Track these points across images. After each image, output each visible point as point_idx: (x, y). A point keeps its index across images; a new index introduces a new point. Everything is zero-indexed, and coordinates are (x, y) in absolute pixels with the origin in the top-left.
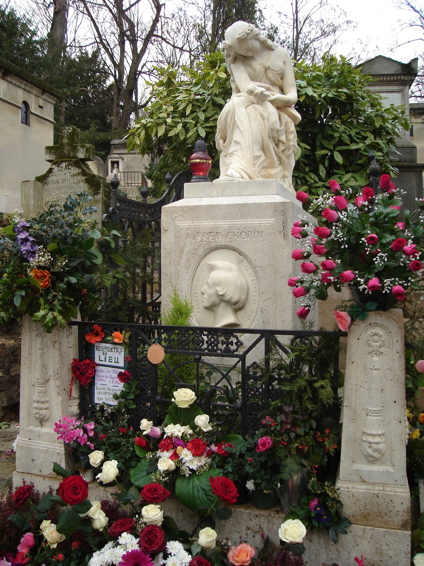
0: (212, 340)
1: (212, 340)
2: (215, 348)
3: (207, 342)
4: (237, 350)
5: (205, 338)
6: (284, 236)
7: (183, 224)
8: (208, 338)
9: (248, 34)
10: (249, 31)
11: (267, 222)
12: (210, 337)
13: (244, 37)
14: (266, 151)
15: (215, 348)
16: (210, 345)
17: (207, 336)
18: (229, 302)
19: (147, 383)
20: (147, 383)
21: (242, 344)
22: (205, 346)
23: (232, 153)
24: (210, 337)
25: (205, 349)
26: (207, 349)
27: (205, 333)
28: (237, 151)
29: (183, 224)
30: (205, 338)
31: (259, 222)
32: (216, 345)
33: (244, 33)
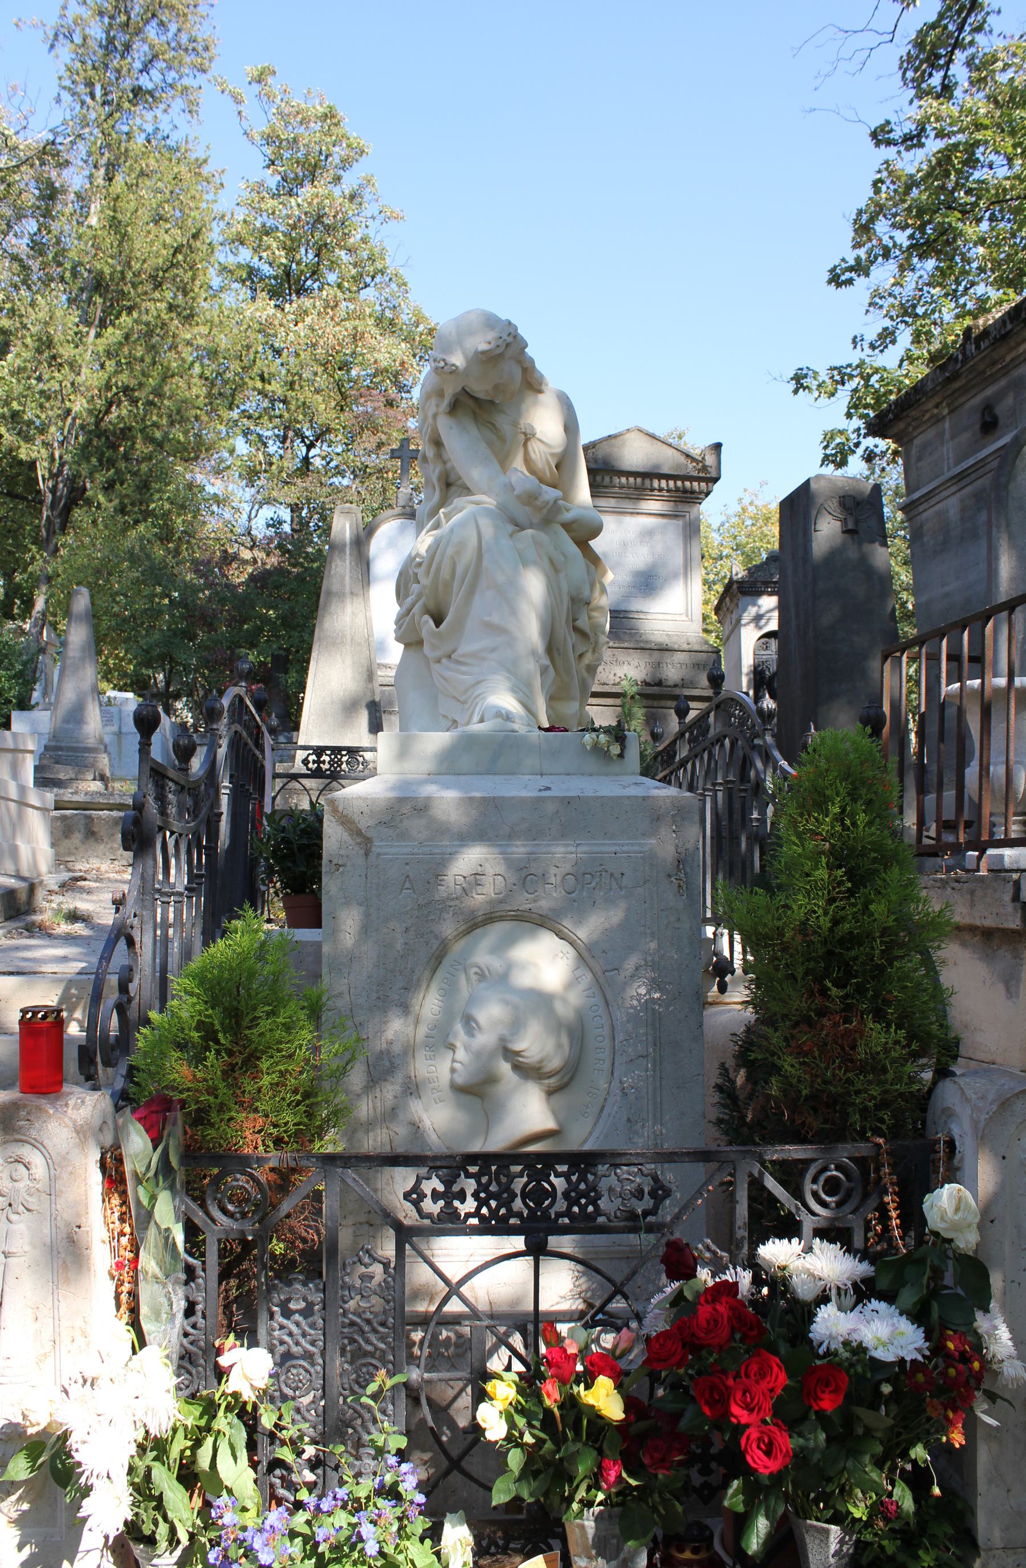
0: (583, 1186)
1: (583, 1186)
2: (590, 1208)
3: (566, 1195)
4: (653, 1212)
5: (560, 1183)
6: (679, 886)
7: (393, 850)
8: (568, 1180)
9: (508, 345)
10: (510, 339)
11: (636, 848)
12: (574, 1178)
13: (499, 351)
14: (556, 654)
15: (590, 1208)
16: (577, 1203)
17: (567, 1176)
18: (540, 1068)
19: (375, 1331)
20: (375, 1331)
21: (668, 1193)
22: (561, 1205)
23: (473, 655)
24: (574, 1178)
25: (559, 1215)
26: (568, 1213)
27: (563, 1168)
28: (493, 650)
29: (393, 850)
30: (560, 1183)
31: (614, 849)
32: (594, 1202)
33: (500, 342)
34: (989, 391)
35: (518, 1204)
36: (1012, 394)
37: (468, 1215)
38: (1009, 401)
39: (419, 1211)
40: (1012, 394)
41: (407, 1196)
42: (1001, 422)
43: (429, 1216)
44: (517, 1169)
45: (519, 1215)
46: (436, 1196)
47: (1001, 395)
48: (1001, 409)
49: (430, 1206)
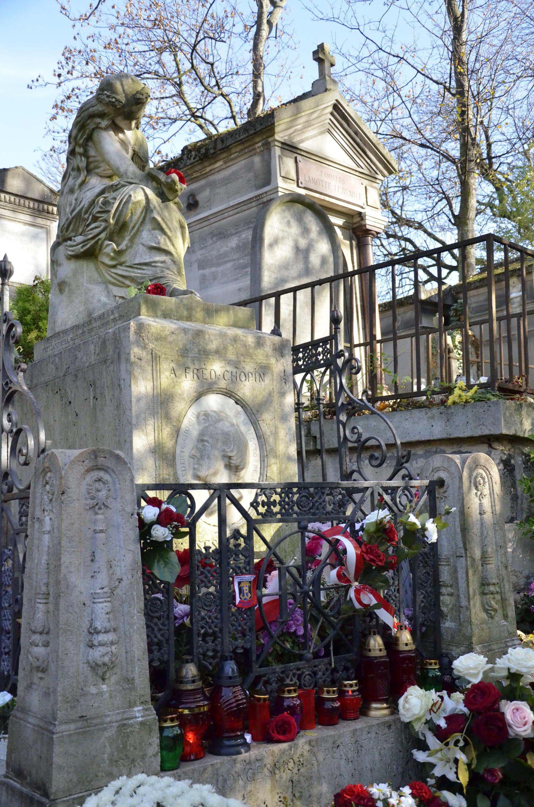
34: (194, 186)
35: (296, 508)
36: (208, 190)
37: (277, 513)
38: (206, 193)
39: (257, 511)
40: (208, 190)
41: (252, 505)
42: (201, 204)
43: (261, 514)
44: (295, 490)
45: (296, 513)
46: (263, 504)
47: (202, 189)
48: (201, 198)
49: (261, 509)
